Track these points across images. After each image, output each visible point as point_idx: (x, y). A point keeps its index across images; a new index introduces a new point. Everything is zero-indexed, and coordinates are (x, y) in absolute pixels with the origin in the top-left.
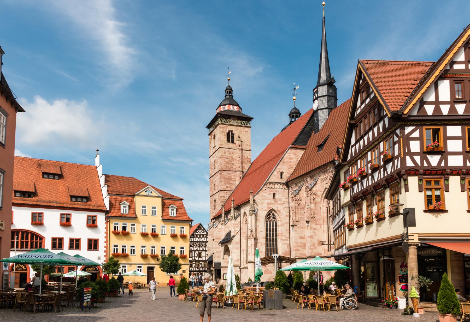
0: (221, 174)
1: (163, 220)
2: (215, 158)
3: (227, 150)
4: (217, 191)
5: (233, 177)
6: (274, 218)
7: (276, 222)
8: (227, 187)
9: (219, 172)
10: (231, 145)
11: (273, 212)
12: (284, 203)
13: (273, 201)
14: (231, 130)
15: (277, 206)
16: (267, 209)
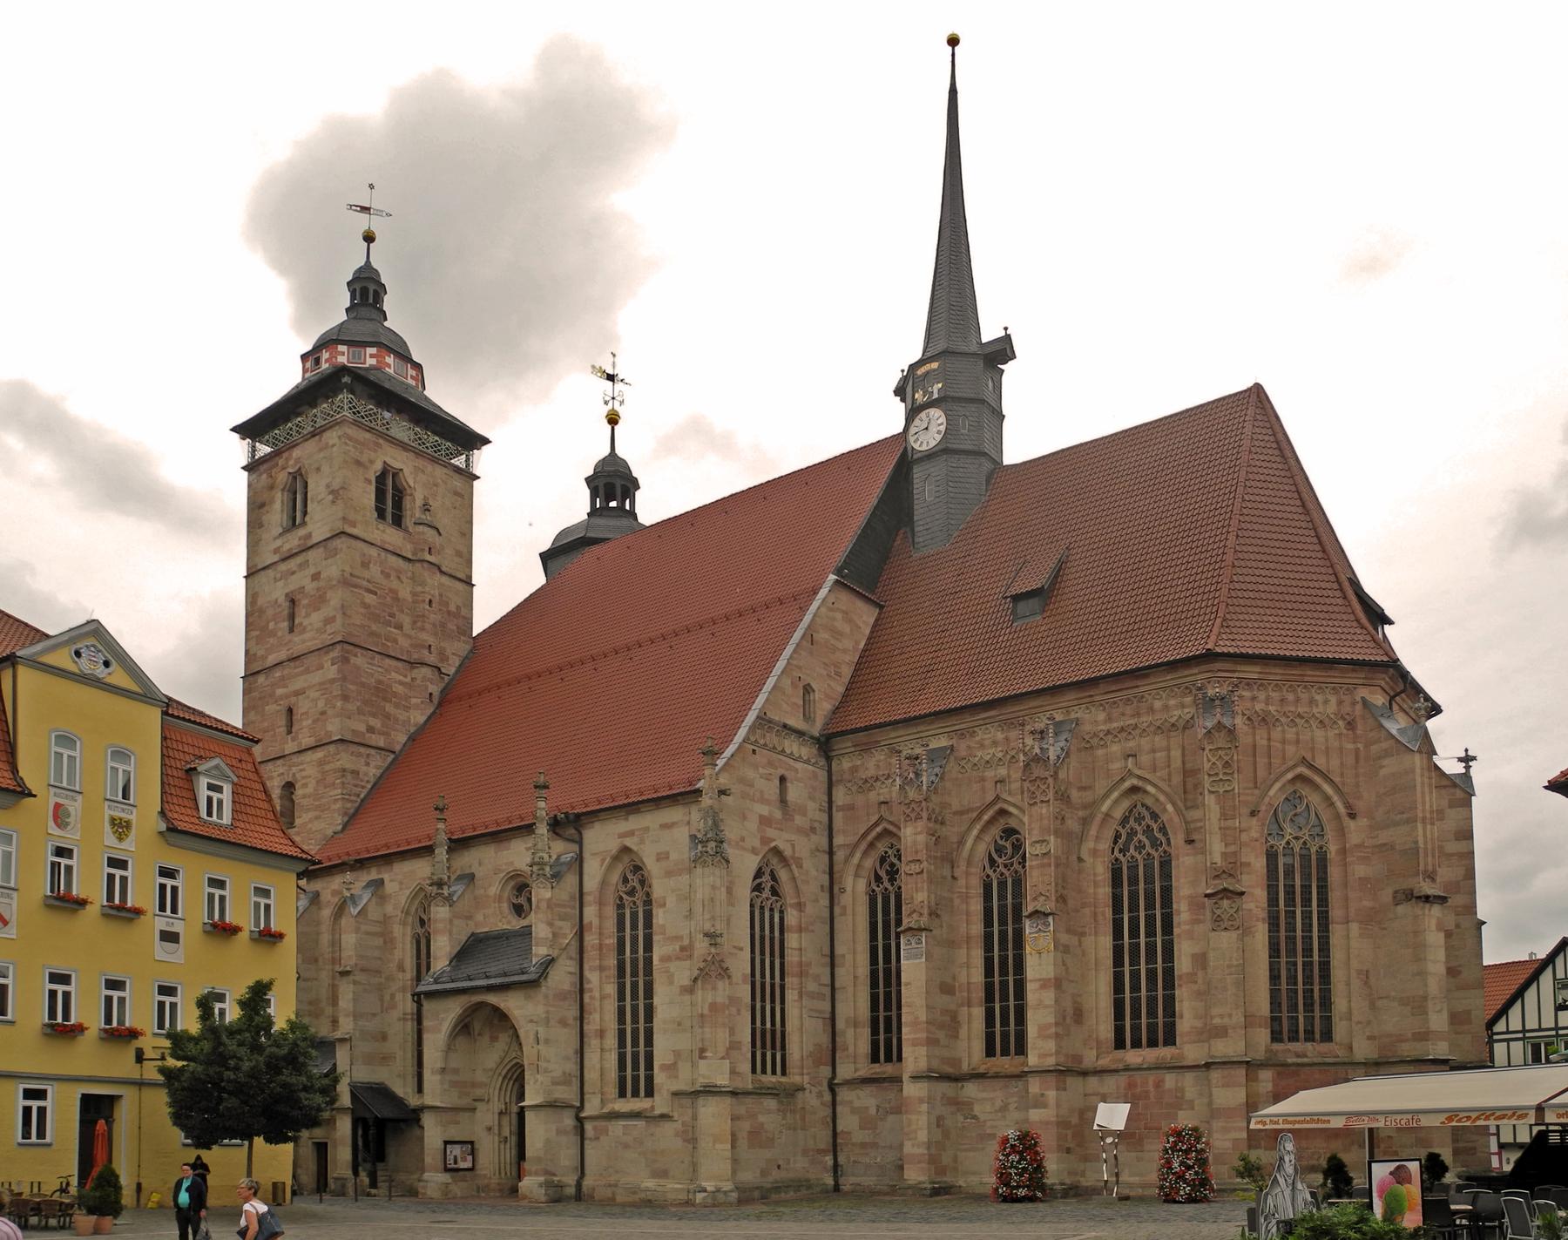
0: (345, 660)
1: (172, 832)
2: (302, 580)
3: (373, 552)
4: (307, 741)
5: (400, 689)
6: (774, 892)
7: (781, 912)
8: (371, 730)
9: (336, 653)
10: (389, 535)
11: (774, 861)
12: (813, 830)
13: (778, 814)
14: (397, 465)
15: (793, 837)
16: (757, 843)
